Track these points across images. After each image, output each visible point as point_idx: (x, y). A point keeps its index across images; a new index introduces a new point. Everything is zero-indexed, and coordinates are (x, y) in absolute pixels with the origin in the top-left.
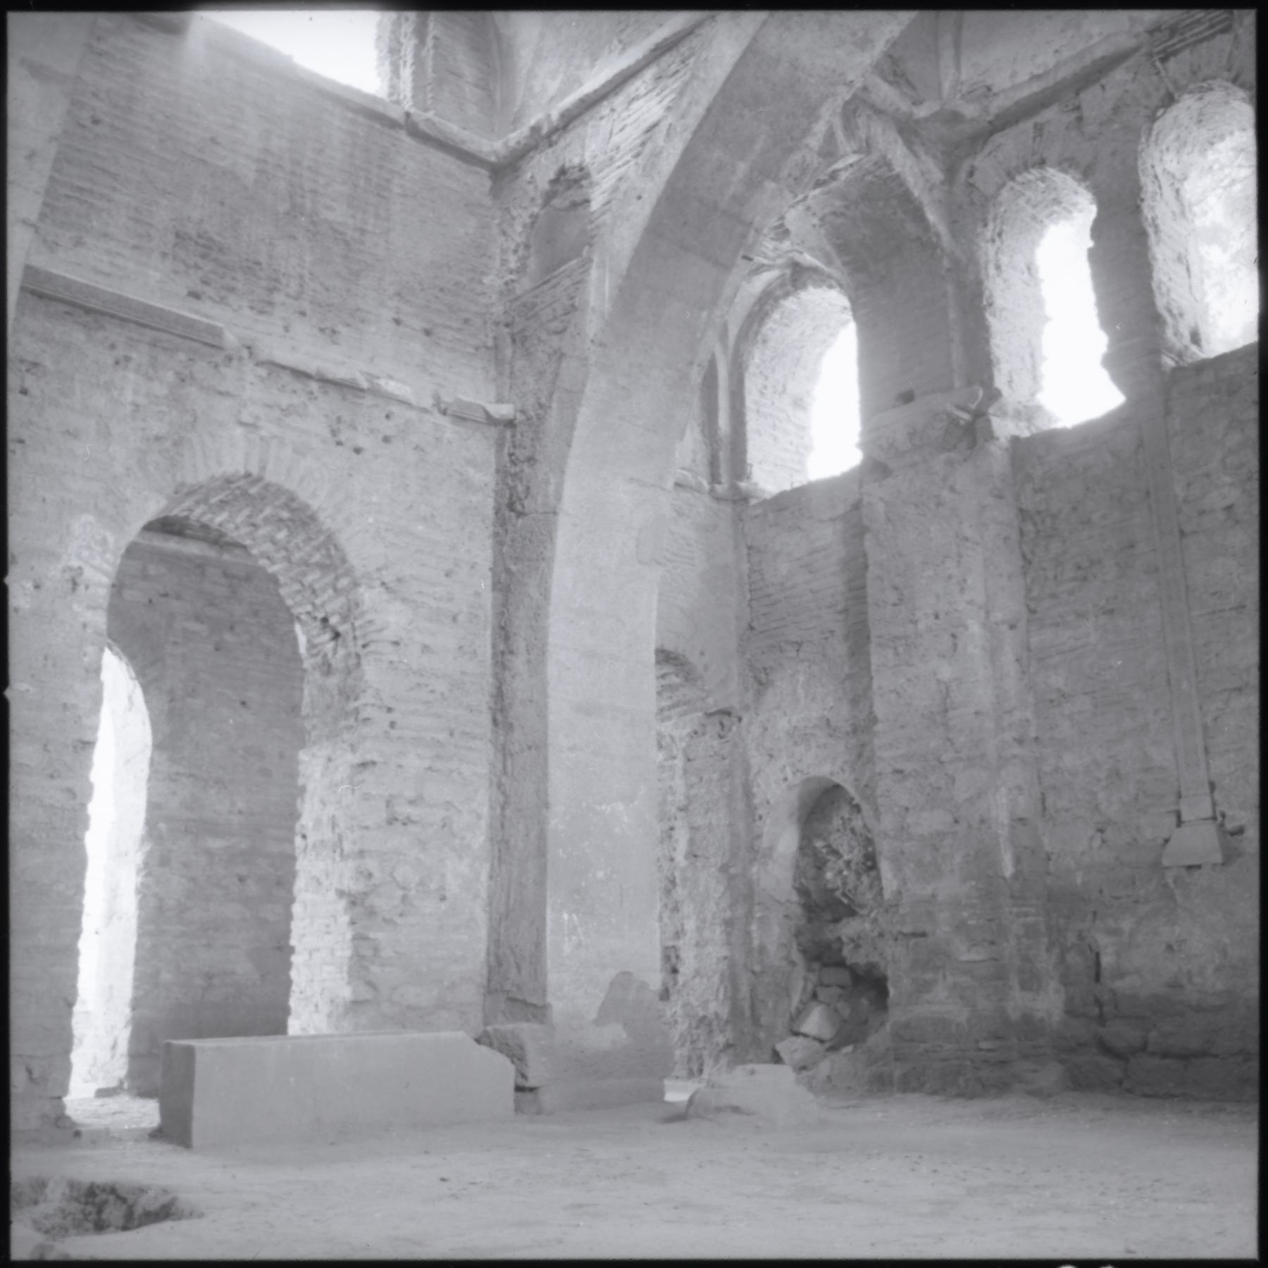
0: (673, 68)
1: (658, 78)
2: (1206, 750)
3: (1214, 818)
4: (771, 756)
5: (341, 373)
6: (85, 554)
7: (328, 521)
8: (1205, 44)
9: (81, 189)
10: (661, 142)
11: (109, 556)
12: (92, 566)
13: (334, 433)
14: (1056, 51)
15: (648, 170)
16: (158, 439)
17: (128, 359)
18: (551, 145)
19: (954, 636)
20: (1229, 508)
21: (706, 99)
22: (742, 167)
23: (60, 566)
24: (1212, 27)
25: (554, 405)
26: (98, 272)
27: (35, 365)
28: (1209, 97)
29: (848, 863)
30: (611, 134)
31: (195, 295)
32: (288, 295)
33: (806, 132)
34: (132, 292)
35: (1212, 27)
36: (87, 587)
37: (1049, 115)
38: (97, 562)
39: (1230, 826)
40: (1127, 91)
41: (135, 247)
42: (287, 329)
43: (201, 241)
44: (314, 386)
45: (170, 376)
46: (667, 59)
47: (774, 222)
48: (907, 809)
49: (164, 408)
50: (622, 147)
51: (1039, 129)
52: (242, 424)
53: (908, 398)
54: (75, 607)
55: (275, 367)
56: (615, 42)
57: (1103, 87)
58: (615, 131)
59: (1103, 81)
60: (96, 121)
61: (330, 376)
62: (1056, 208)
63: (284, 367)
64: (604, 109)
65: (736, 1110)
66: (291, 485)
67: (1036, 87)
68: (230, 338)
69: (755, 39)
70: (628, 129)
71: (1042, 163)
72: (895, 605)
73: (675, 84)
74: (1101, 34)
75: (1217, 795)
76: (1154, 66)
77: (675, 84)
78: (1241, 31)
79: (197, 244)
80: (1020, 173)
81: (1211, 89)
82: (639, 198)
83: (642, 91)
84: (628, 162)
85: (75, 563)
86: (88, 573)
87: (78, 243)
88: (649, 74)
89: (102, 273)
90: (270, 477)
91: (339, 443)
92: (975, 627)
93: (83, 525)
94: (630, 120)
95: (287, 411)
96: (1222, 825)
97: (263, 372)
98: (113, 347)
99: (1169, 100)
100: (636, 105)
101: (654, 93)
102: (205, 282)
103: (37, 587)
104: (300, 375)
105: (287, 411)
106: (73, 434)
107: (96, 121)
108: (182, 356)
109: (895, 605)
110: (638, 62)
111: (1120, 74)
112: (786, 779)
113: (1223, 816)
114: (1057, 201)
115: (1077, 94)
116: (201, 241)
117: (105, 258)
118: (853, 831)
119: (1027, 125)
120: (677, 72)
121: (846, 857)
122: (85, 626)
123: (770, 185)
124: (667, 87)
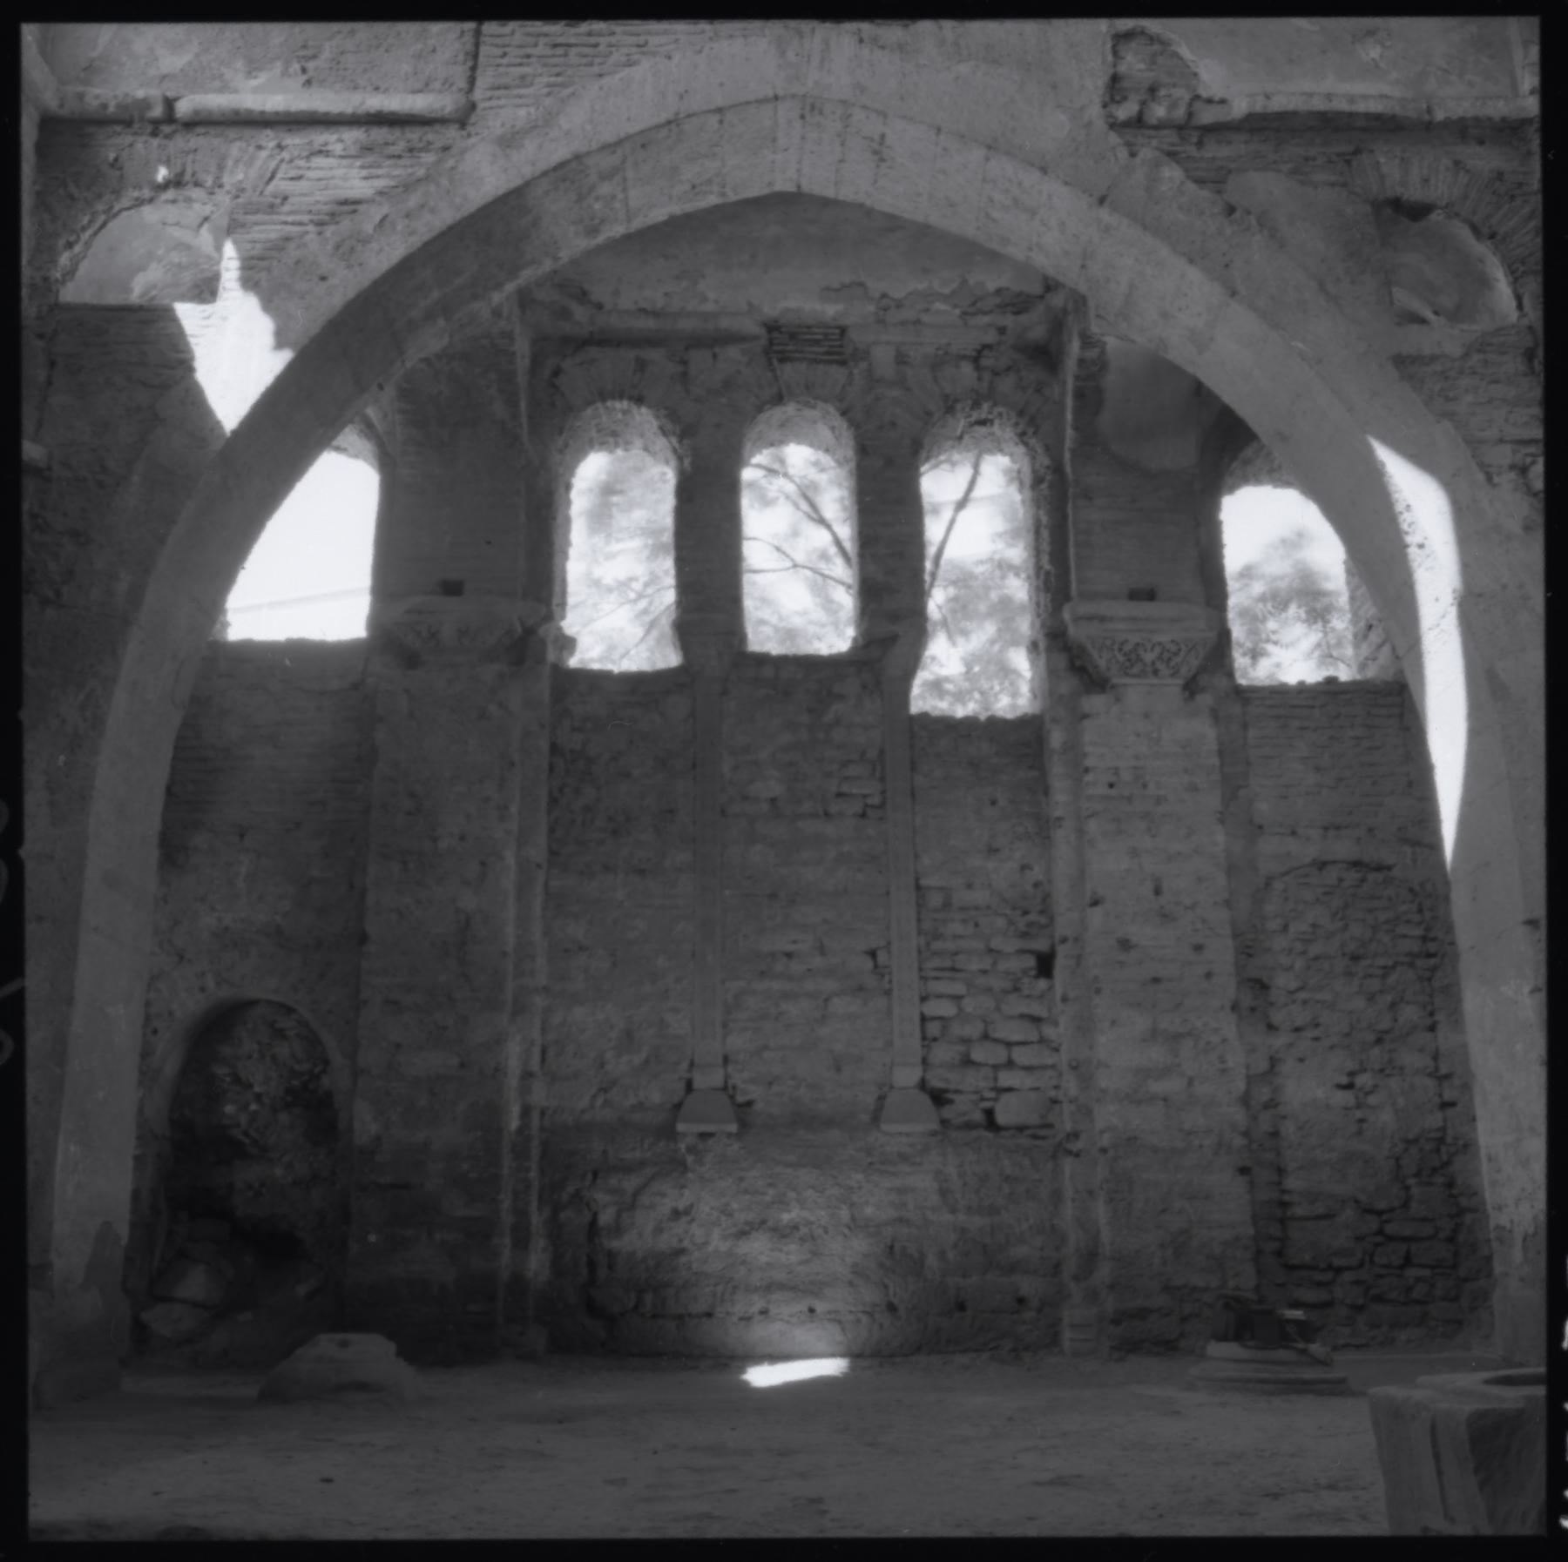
0: (392, 150)
1: (367, 149)
2: (725, 1026)
3: (725, 1088)
4: (182, 958)
8: (821, 367)
10: (368, 228)
14: (666, 294)
15: (347, 250)
18: (154, 134)
19: (483, 864)
20: (773, 800)
21: (446, 216)
22: (436, 294)
24: (827, 353)
25: (136, 479)
28: (809, 413)
29: (258, 1097)
30: (272, 177)
33: (498, 286)
35: (827, 353)
37: (654, 355)
39: (740, 1099)
40: (739, 372)
46: (380, 134)
47: (72, 239)
48: (398, 1046)
50: (291, 200)
51: (642, 365)
53: (452, 589)
56: (296, 66)
57: (715, 356)
58: (280, 175)
59: (717, 350)
62: (611, 440)
64: (268, 138)
65: (362, 1387)
67: (650, 324)
69: (527, 184)
70: (303, 183)
71: (639, 400)
72: (409, 813)
73: (400, 171)
74: (716, 302)
75: (730, 1069)
76: (770, 364)
77: (400, 171)
78: (856, 371)
80: (613, 398)
81: (814, 407)
82: (323, 278)
83: (338, 148)
84: (301, 224)
88: (353, 135)
92: (510, 858)
94: (310, 174)
96: (732, 1097)
99: (779, 399)
100: (319, 161)
101: (358, 163)
109: (409, 813)
110: (340, 114)
111: (733, 352)
112: (203, 989)
113: (734, 1088)
114: (614, 434)
115: (687, 349)
118: (274, 1058)
119: (632, 354)
120: (400, 157)
121: (257, 1089)
123: (441, 322)
124: (379, 167)
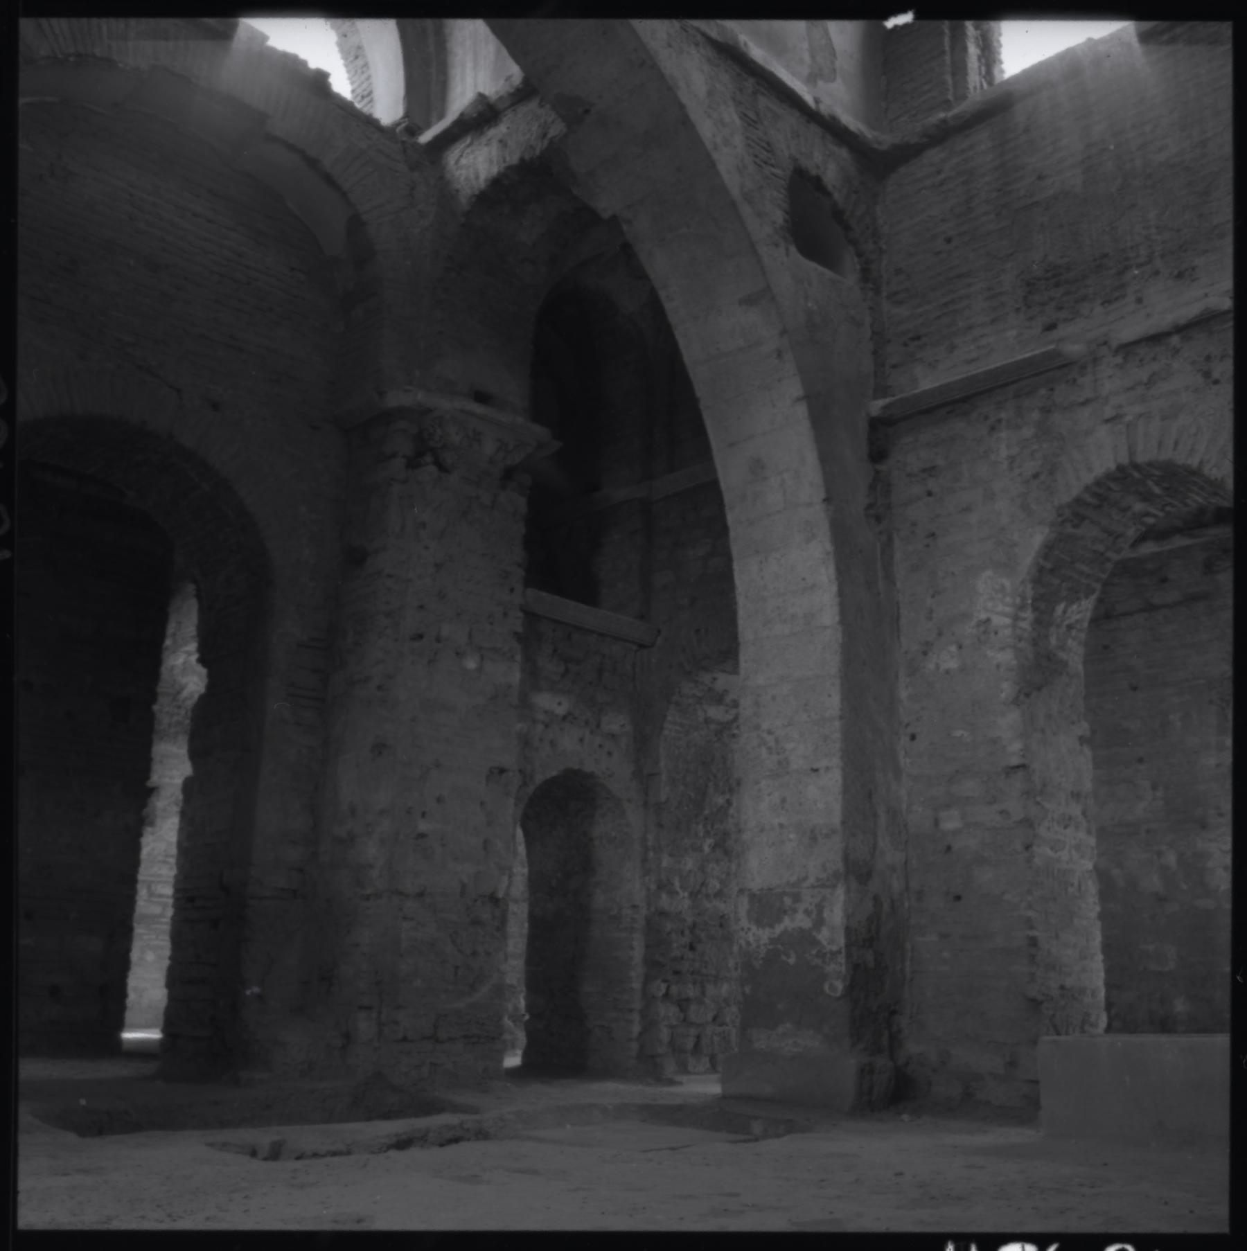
5: (1191, 311)
6: (990, 605)
7: (1214, 471)
9: (946, 305)
11: (1008, 599)
12: (998, 613)
13: (1207, 375)
16: (1036, 476)
17: (999, 421)
23: (973, 623)
26: (969, 362)
27: (933, 468)
31: (1051, 327)
32: (1139, 266)
34: (997, 361)
36: (996, 633)
38: (1000, 608)
41: (993, 321)
42: (1139, 301)
43: (1049, 274)
44: (1175, 340)
45: (1036, 415)
49: (1035, 447)
52: (1107, 421)
54: (990, 653)
55: (1127, 349)
60: (949, 240)
61: (1183, 322)
63: (1137, 343)
66: (1166, 455)
68: (1074, 349)
79: (1047, 279)
85: (983, 616)
86: (997, 620)
87: (952, 348)
89: (973, 360)
90: (1141, 459)
91: (1216, 382)
93: (985, 582)
95: (1150, 383)
97: (1119, 360)
98: (986, 418)
102: (1060, 308)
103: (960, 647)
104: (1156, 339)
105: (1150, 383)
106: (968, 509)
107: (949, 240)
108: (1043, 391)
116: (1049, 274)
117: (972, 347)
122: (998, 666)
